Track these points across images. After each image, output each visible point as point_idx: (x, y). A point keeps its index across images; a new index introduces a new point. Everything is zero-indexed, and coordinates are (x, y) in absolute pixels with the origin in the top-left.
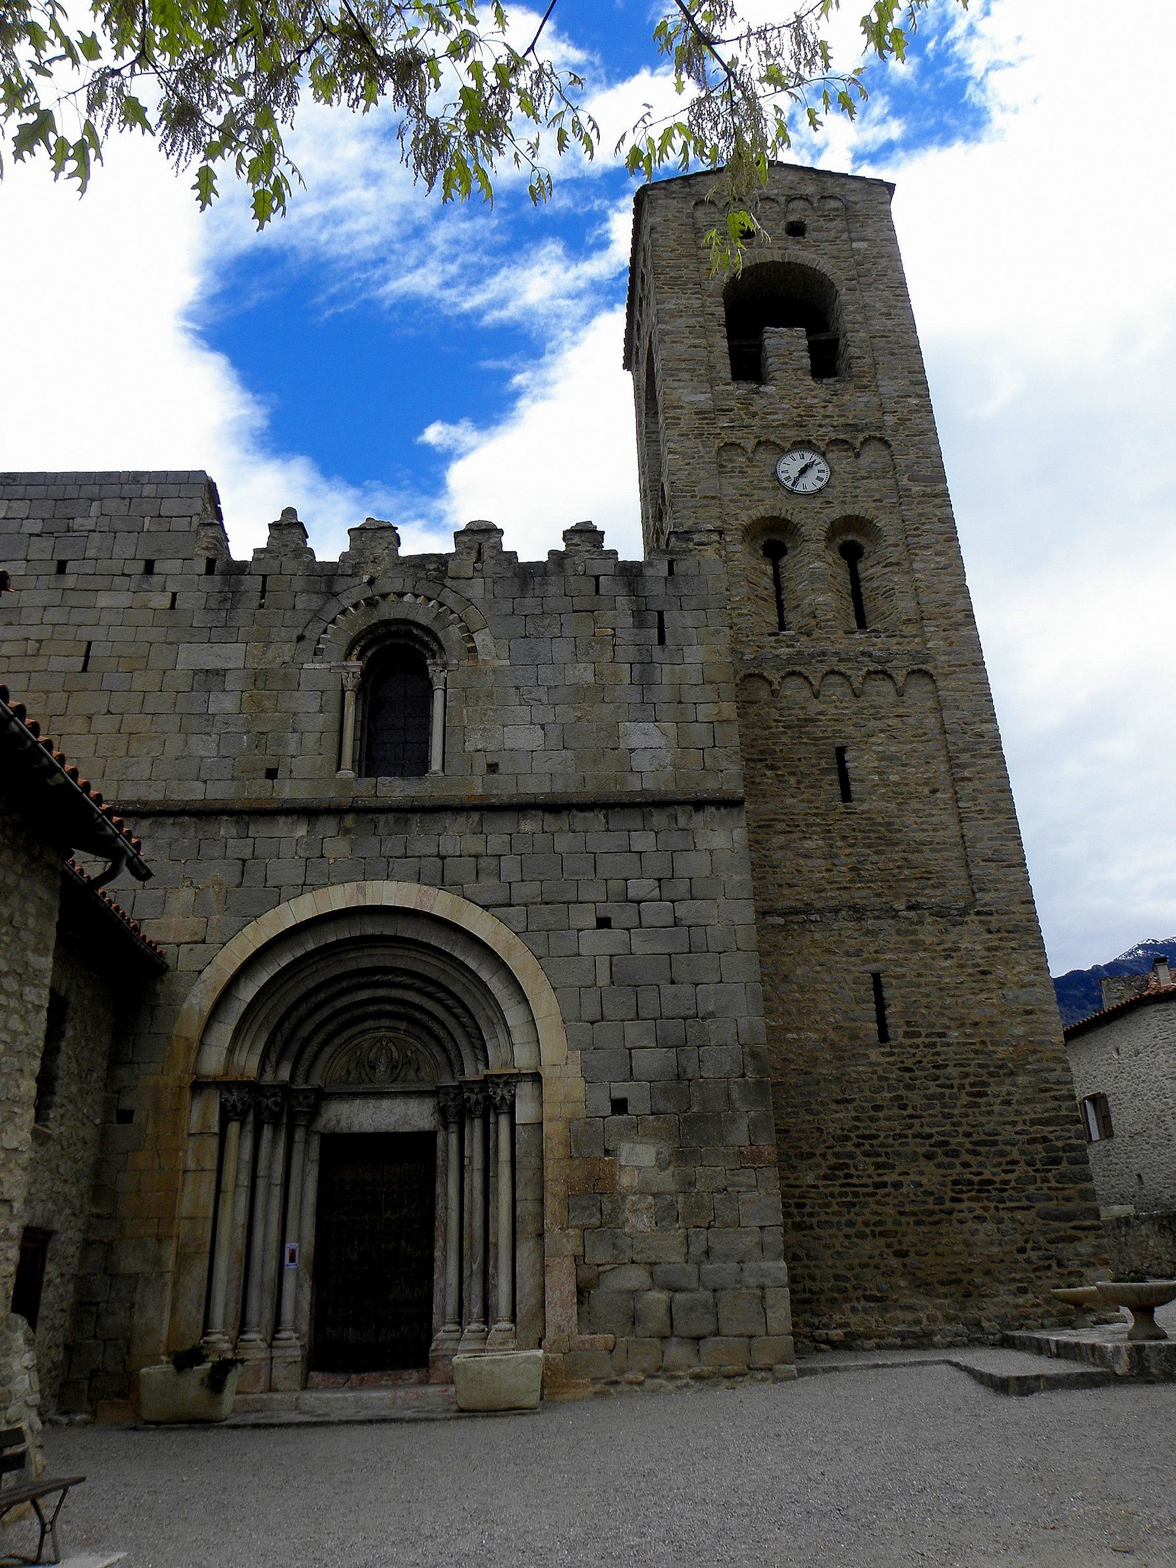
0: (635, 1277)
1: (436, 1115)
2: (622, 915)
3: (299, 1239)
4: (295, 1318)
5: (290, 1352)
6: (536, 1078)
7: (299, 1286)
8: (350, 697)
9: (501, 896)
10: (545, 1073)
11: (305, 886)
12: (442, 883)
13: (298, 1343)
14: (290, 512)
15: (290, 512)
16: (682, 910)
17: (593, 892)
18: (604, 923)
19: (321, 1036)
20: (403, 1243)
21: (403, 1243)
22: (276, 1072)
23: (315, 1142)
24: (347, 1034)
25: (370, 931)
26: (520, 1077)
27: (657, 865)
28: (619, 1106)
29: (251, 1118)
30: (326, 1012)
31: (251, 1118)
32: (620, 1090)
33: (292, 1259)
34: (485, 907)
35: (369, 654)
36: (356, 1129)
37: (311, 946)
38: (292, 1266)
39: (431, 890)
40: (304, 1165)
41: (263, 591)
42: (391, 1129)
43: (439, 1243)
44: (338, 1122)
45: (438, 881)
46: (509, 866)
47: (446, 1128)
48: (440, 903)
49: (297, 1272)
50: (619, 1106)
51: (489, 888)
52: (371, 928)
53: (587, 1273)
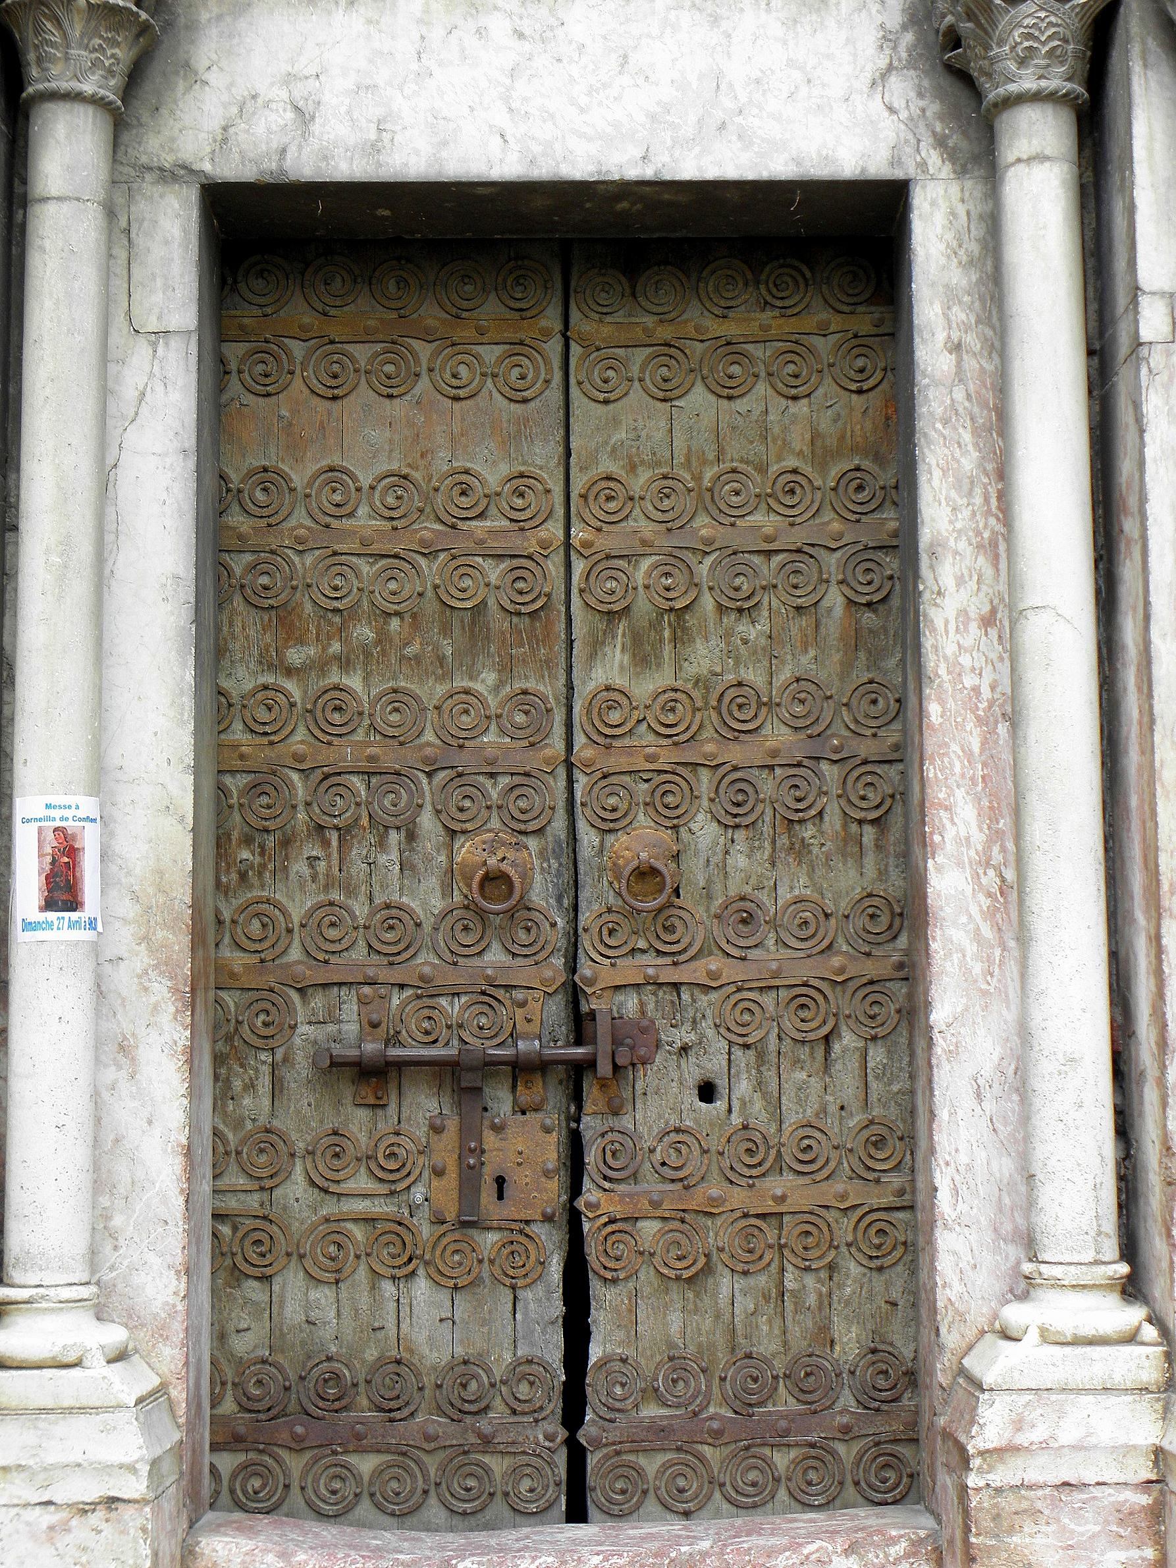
1: (902, 89)
3: (100, 776)
4: (101, 1233)
5: (73, 1441)
7: (113, 1049)
13: (128, 1383)
20: (704, 831)
21: (704, 831)
33: (62, 891)
36: (413, 157)
38: (63, 930)
40: (106, 359)
42: (625, 162)
43: (956, 825)
44: (304, 116)
47: (977, 138)
49: (100, 962)
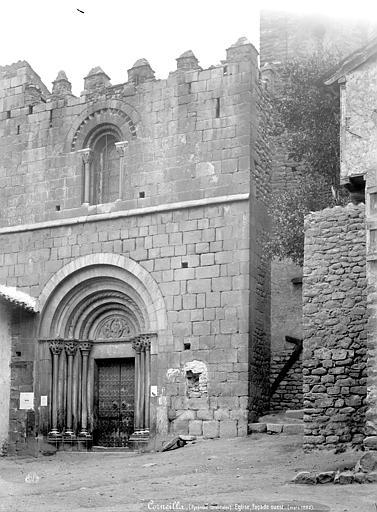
0: (190, 414)
2: (192, 261)
6: (156, 335)
8: (87, 166)
9: (144, 256)
10: (160, 333)
11: (72, 258)
12: (122, 251)
14: (62, 73)
15: (62, 73)
16: (219, 257)
17: (180, 250)
18: (185, 265)
19: (90, 320)
22: (74, 335)
23: (92, 363)
24: (102, 318)
25: (97, 275)
26: (149, 336)
27: (208, 234)
28: (187, 347)
29: (63, 353)
30: (91, 309)
31: (63, 353)
32: (188, 341)
34: (138, 262)
35: (98, 138)
37: (76, 283)
39: (117, 256)
41: (51, 119)
45: (120, 250)
46: (148, 240)
48: (118, 260)
50: (187, 347)
51: (140, 254)
52: (97, 273)
53: (171, 413)
